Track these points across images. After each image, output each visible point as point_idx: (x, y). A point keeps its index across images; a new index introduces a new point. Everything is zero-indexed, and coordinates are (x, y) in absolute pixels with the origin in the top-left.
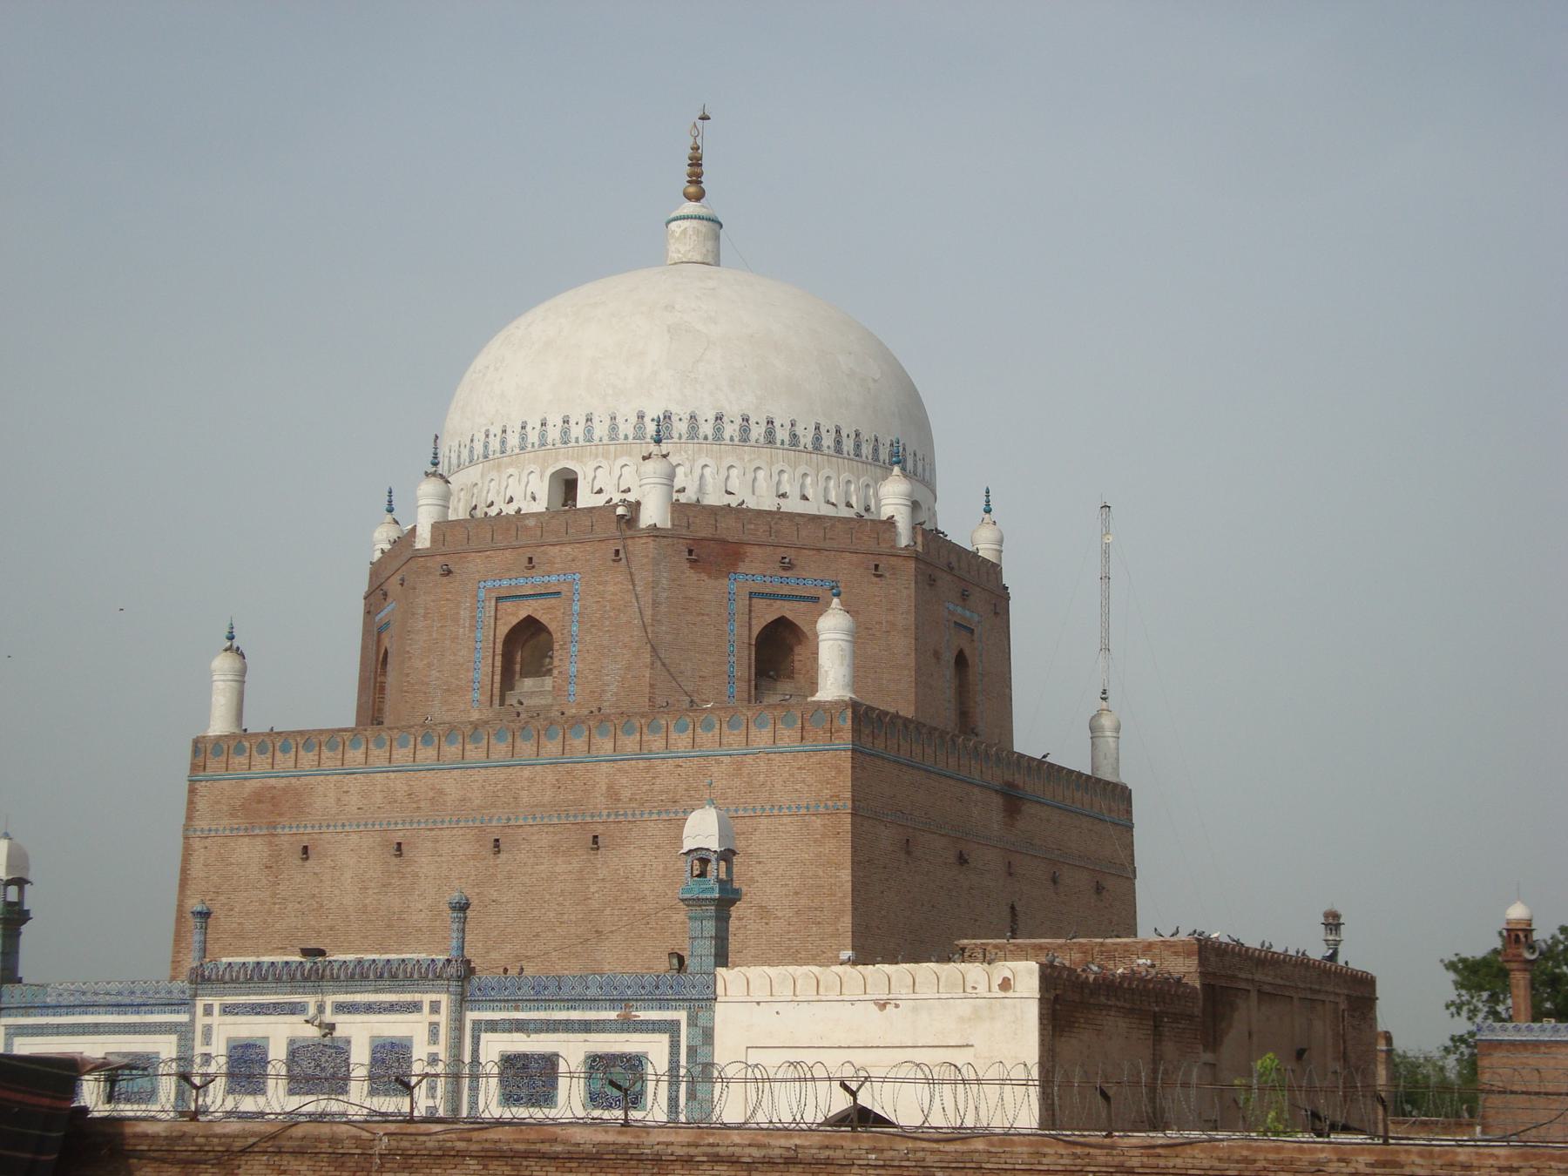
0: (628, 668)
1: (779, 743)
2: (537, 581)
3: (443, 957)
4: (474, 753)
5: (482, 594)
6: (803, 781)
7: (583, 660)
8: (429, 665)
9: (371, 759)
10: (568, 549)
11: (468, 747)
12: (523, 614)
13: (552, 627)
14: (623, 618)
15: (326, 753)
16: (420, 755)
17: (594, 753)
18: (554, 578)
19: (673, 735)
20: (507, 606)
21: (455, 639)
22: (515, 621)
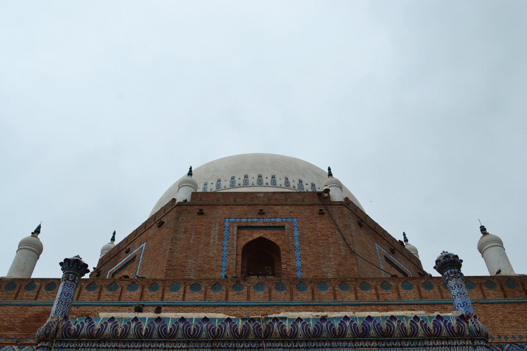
0: (340, 264)
1: (488, 298)
2: (267, 221)
3: (452, 315)
4: (234, 297)
5: (227, 224)
6: (517, 321)
7: (306, 259)
8: (186, 257)
9: (145, 298)
10: (287, 207)
11: (230, 293)
12: (257, 235)
13: (278, 243)
14: (331, 240)
15: (105, 292)
16: (187, 296)
17: (339, 299)
18: (278, 220)
19: (403, 292)
20: (246, 232)
21: (207, 244)
22: (250, 239)
